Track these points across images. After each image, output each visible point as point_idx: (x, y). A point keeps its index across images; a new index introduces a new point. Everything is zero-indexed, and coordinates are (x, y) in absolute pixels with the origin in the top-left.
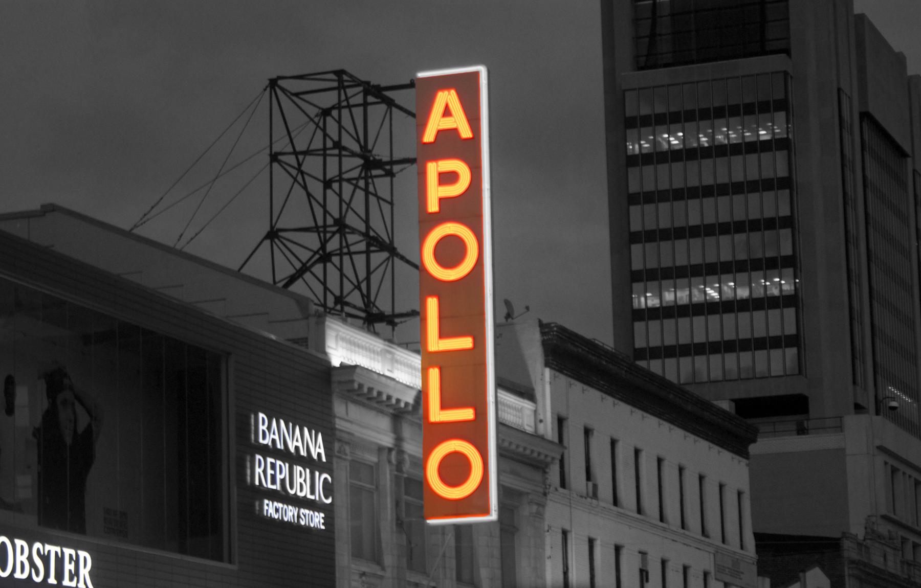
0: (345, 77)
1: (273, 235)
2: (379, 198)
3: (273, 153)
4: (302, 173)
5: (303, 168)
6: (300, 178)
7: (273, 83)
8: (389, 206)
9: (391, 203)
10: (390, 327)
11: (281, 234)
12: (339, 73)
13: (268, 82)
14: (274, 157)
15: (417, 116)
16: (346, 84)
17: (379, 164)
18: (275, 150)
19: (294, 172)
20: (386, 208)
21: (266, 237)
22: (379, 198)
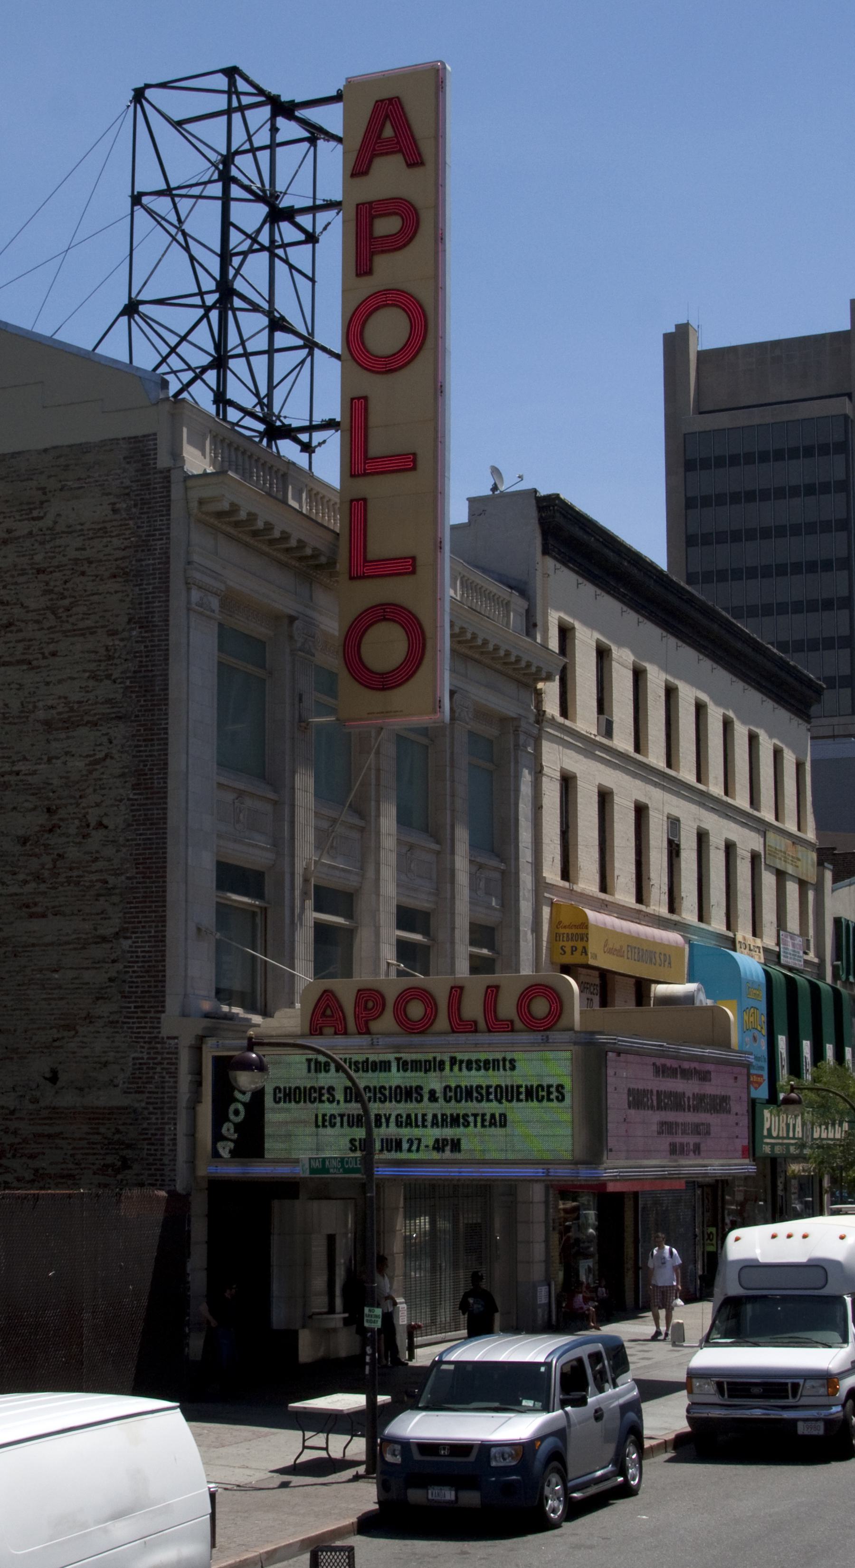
0: (242, 85)
1: (131, 309)
2: (291, 267)
3: (136, 193)
4: (185, 234)
5: (185, 227)
6: (180, 237)
7: (139, 95)
8: (310, 284)
9: (312, 280)
10: (306, 455)
11: (142, 308)
12: (231, 73)
13: (132, 93)
14: (136, 199)
15: (344, 140)
16: (246, 100)
17: (289, 215)
18: (138, 189)
19: (173, 231)
20: (304, 285)
21: (122, 314)
22: (291, 267)
